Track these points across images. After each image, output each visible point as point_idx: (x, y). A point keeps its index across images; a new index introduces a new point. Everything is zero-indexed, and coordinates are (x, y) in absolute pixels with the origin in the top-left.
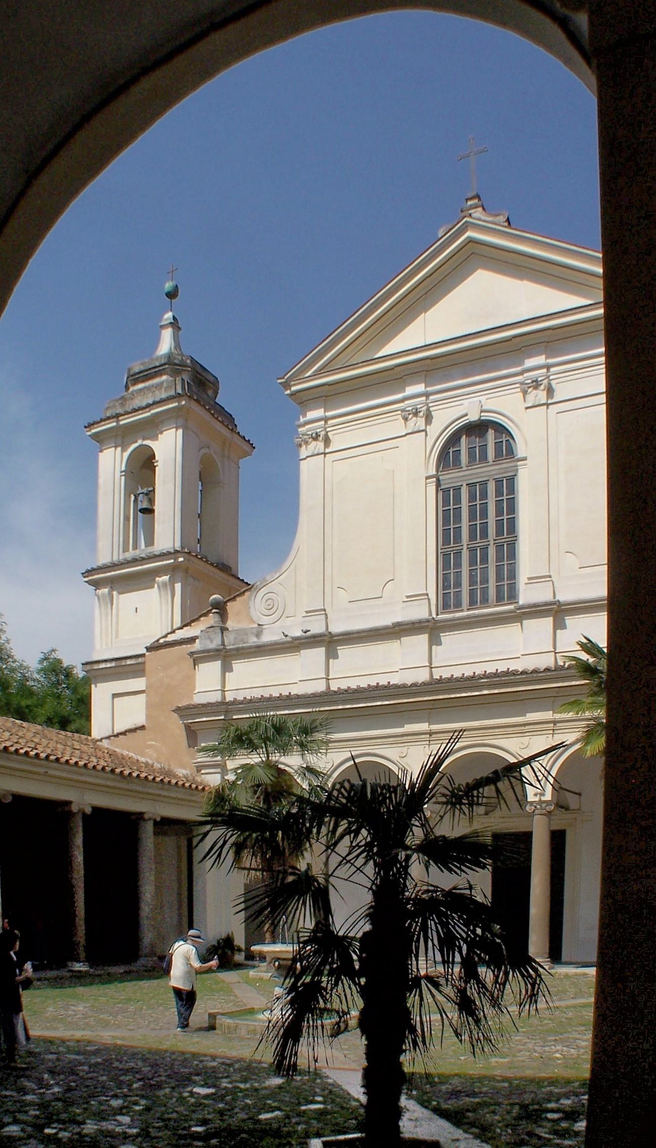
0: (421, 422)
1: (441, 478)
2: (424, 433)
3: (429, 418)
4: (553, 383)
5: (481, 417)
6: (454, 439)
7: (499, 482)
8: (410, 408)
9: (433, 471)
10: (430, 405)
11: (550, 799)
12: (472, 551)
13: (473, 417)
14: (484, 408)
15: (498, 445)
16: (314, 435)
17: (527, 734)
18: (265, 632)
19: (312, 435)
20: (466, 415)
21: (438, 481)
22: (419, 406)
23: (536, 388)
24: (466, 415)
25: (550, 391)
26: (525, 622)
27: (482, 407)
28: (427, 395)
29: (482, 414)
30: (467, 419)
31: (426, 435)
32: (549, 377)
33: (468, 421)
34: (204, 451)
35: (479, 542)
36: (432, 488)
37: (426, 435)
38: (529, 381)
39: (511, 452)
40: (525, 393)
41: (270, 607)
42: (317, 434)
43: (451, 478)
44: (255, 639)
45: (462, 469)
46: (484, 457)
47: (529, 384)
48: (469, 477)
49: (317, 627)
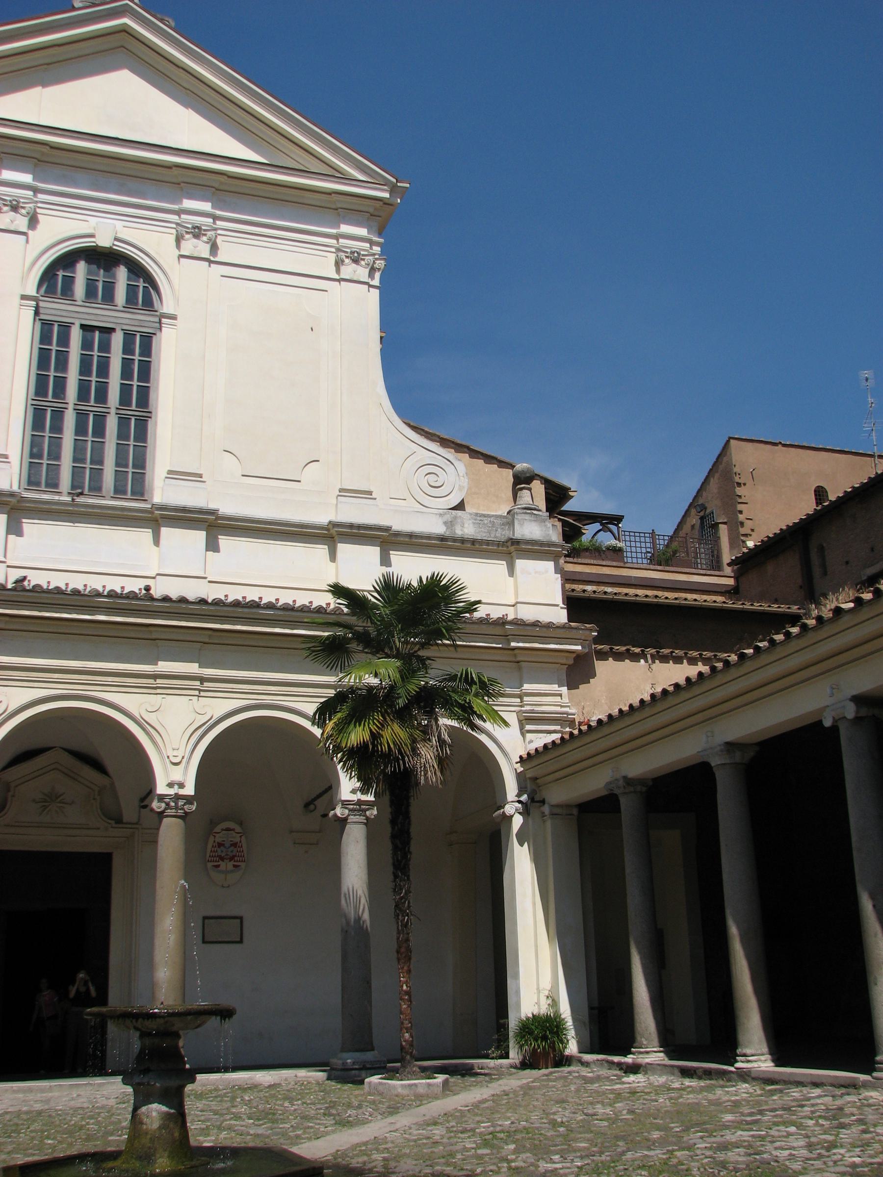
0: (21, 223)
1: (41, 304)
2: (24, 237)
3: (33, 221)
4: (219, 240)
6: (67, 260)
7: (129, 337)
9: (32, 290)
10: (40, 205)
11: (192, 793)
13: (104, 241)
14: (120, 235)
15: (131, 291)
17: (159, 691)
20: (92, 236)
22: (22, 200)
23: (197, 236)
24: (92, 236)
25: (214, 248)
26: (165, 531)
27: (116, 234)
29: (116, 243)
30: (94, 242)
31: (27, 241)
33: (94, 244)
37: (27, 241)
38: (190, 226)
39: (148, 304)
40: (179, 240)
43: (55, 308)
47: (188, 228)
48: (86, 317)
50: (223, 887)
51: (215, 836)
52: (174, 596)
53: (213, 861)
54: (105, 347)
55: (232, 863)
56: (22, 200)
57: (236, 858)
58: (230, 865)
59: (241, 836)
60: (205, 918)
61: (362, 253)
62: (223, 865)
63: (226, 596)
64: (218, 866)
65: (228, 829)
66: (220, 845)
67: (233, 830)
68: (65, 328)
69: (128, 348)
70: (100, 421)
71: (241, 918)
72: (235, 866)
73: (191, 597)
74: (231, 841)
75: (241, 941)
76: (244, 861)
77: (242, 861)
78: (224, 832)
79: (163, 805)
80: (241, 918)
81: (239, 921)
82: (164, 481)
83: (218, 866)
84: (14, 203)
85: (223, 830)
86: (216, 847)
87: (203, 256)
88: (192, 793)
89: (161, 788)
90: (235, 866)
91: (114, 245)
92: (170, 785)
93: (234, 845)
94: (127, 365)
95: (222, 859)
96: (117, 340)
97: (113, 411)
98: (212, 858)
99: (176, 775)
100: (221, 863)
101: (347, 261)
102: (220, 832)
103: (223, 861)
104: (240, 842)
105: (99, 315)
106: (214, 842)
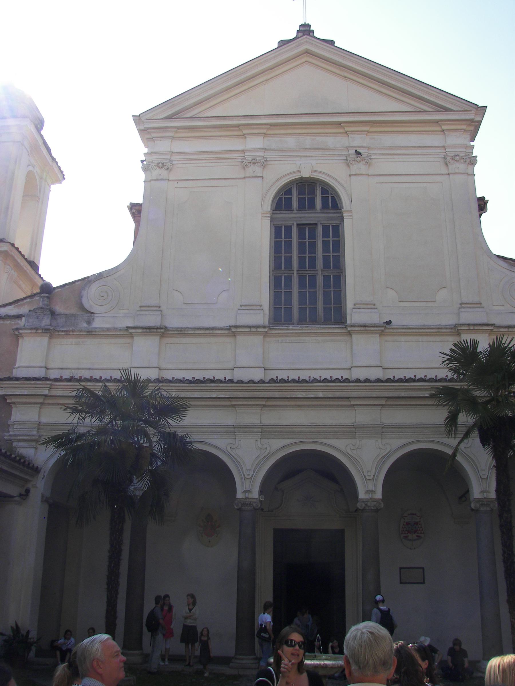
5: (311, 175)
7: (326, 228)
8: (250, 159)
12: (302, 279)
13: (306, 174)
15: (325, 201)
16: (160, 165)
18: (97, 320)
19: (158, 164)
21: (272, 220)
28: (265, 150)
32: (371, 156)
34: (31, 168)
35: (307, 272)
36: (267, 223)
41: (103, 298)
42: (163, 163)
44: (85, 325)
45: (294, 212)
46: (312, 206)
49: (152, 320)
50: (411, 549)
51: (404, 519)
52: (362, 378)
53: (403, 534)
54: (313, 235)
55: (416, 534)
56: (258, 158)
57: (418, 532)
58: (415, 536)
59: (420, 518)
60: (401, 568)
61: (461, 155)
62: (410, 536)
63: (394, 377)
64: (407, 537)
65: (413, 514)
66: (408, 524)
67: (415, 514)
68: (289, 229)
69: (326, 234)
70: (313, 279)
71: (423, 568)
72: (417, 536)
73: (373, 378)
74: (414, 521)
75: (423, 583)
76: (423, 533)
77: (422, 533)
78: (410, 516)
79: (364, 505)
80: (423, 568)
81: (422, 570)
82: (352, 310)
83: (407, 537)
84: (254, 161)
85: (409, 514)
86: (405, 525)
87: (364, 173)
88: (381, 498)
89: (362, 495)
90: (417, 536)
91: (311, 175)
92: (368, 492)
93: (417, 523)
94: (326, 244)
95: (409, 532)
96: (320, 229)
97: (320, 272)
98: (404, 532)
99: (371, 487)
100: (409, 534)
101: (452, 161)
102: (407, 516)
103: (410, 533)
104: (420, 521)
105: (308, 217)
106: (404, 522)
